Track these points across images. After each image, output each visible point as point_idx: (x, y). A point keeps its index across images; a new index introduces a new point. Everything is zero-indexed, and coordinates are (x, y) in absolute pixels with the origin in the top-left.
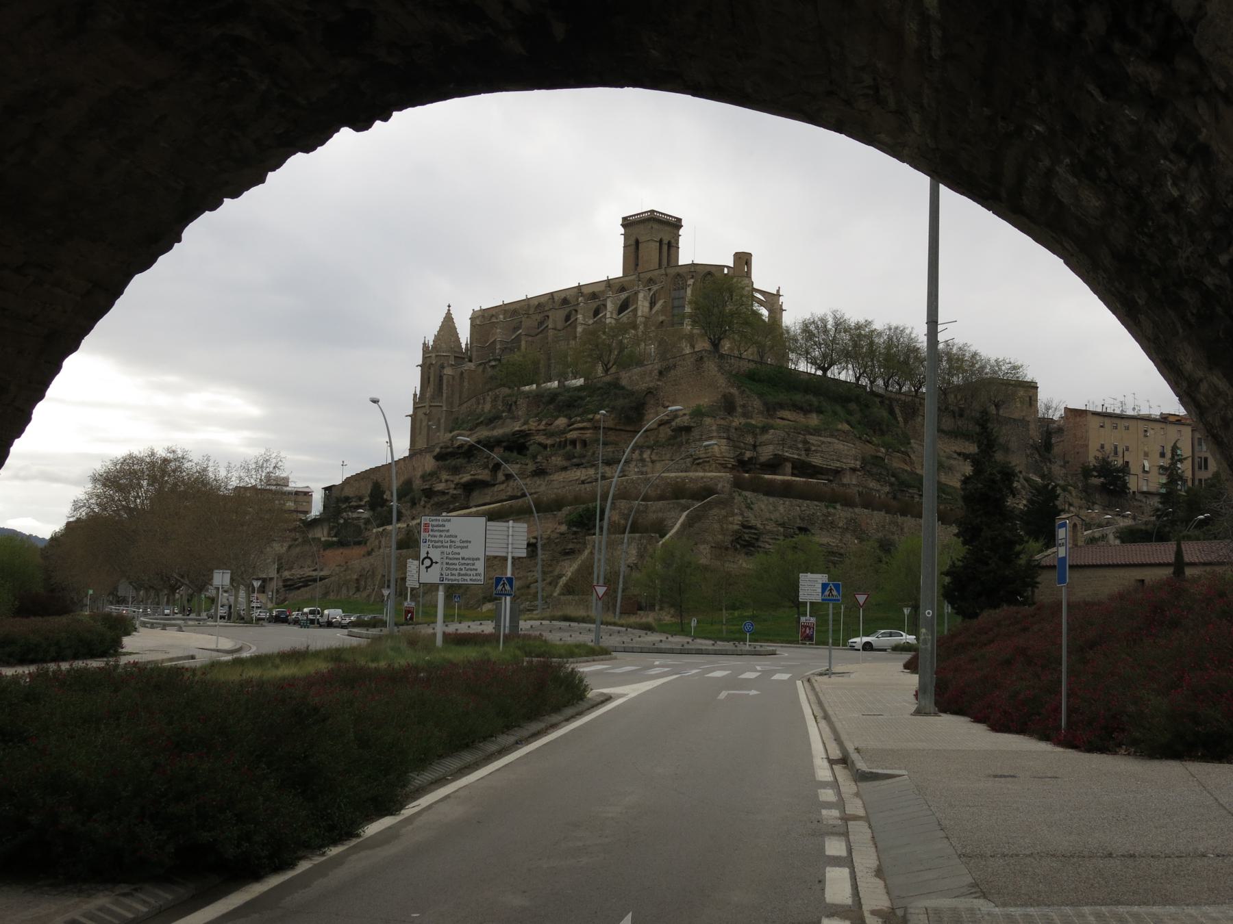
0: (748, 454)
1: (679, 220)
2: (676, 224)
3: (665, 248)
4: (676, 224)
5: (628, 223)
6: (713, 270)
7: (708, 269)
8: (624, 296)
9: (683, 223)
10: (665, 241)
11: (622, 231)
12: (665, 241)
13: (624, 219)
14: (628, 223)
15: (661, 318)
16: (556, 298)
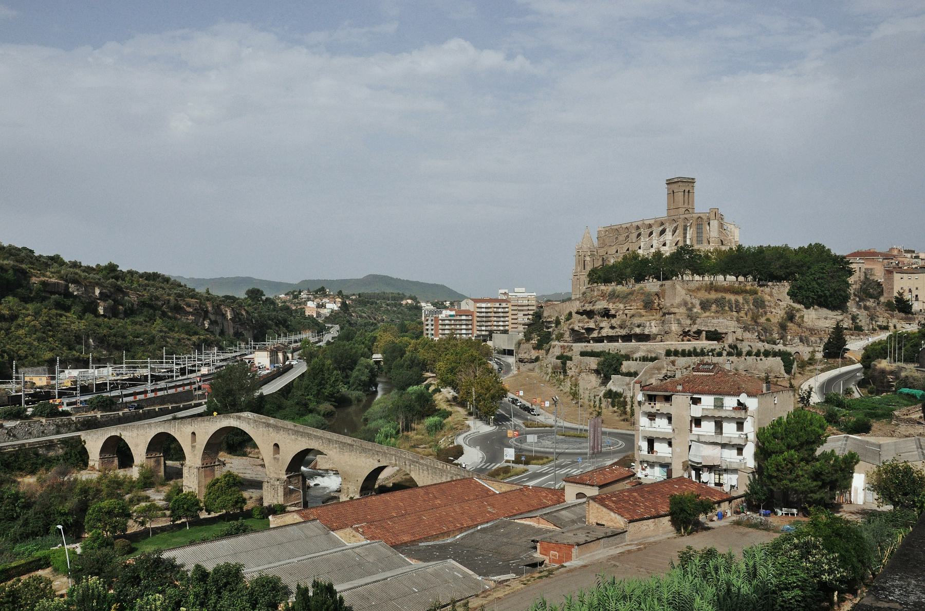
0: (687, 329)
1: (693, 179)
2: (691, 181)
3: (686, 194)
4: (691, 181)
5: (670, 183)
6: (701, 215)
7: (699, 215)
8: (661, 228)
9: (696, 180)
10: (687, 191)
11: (666, 186)
12: (687, 191)
13: (667, 180)
14: (670, 183)
15: (678, 239)
16: (634, 225)
